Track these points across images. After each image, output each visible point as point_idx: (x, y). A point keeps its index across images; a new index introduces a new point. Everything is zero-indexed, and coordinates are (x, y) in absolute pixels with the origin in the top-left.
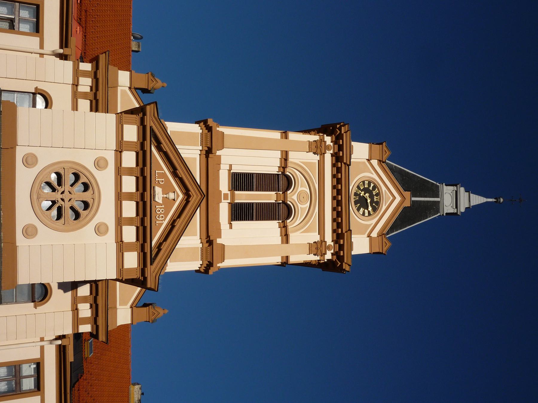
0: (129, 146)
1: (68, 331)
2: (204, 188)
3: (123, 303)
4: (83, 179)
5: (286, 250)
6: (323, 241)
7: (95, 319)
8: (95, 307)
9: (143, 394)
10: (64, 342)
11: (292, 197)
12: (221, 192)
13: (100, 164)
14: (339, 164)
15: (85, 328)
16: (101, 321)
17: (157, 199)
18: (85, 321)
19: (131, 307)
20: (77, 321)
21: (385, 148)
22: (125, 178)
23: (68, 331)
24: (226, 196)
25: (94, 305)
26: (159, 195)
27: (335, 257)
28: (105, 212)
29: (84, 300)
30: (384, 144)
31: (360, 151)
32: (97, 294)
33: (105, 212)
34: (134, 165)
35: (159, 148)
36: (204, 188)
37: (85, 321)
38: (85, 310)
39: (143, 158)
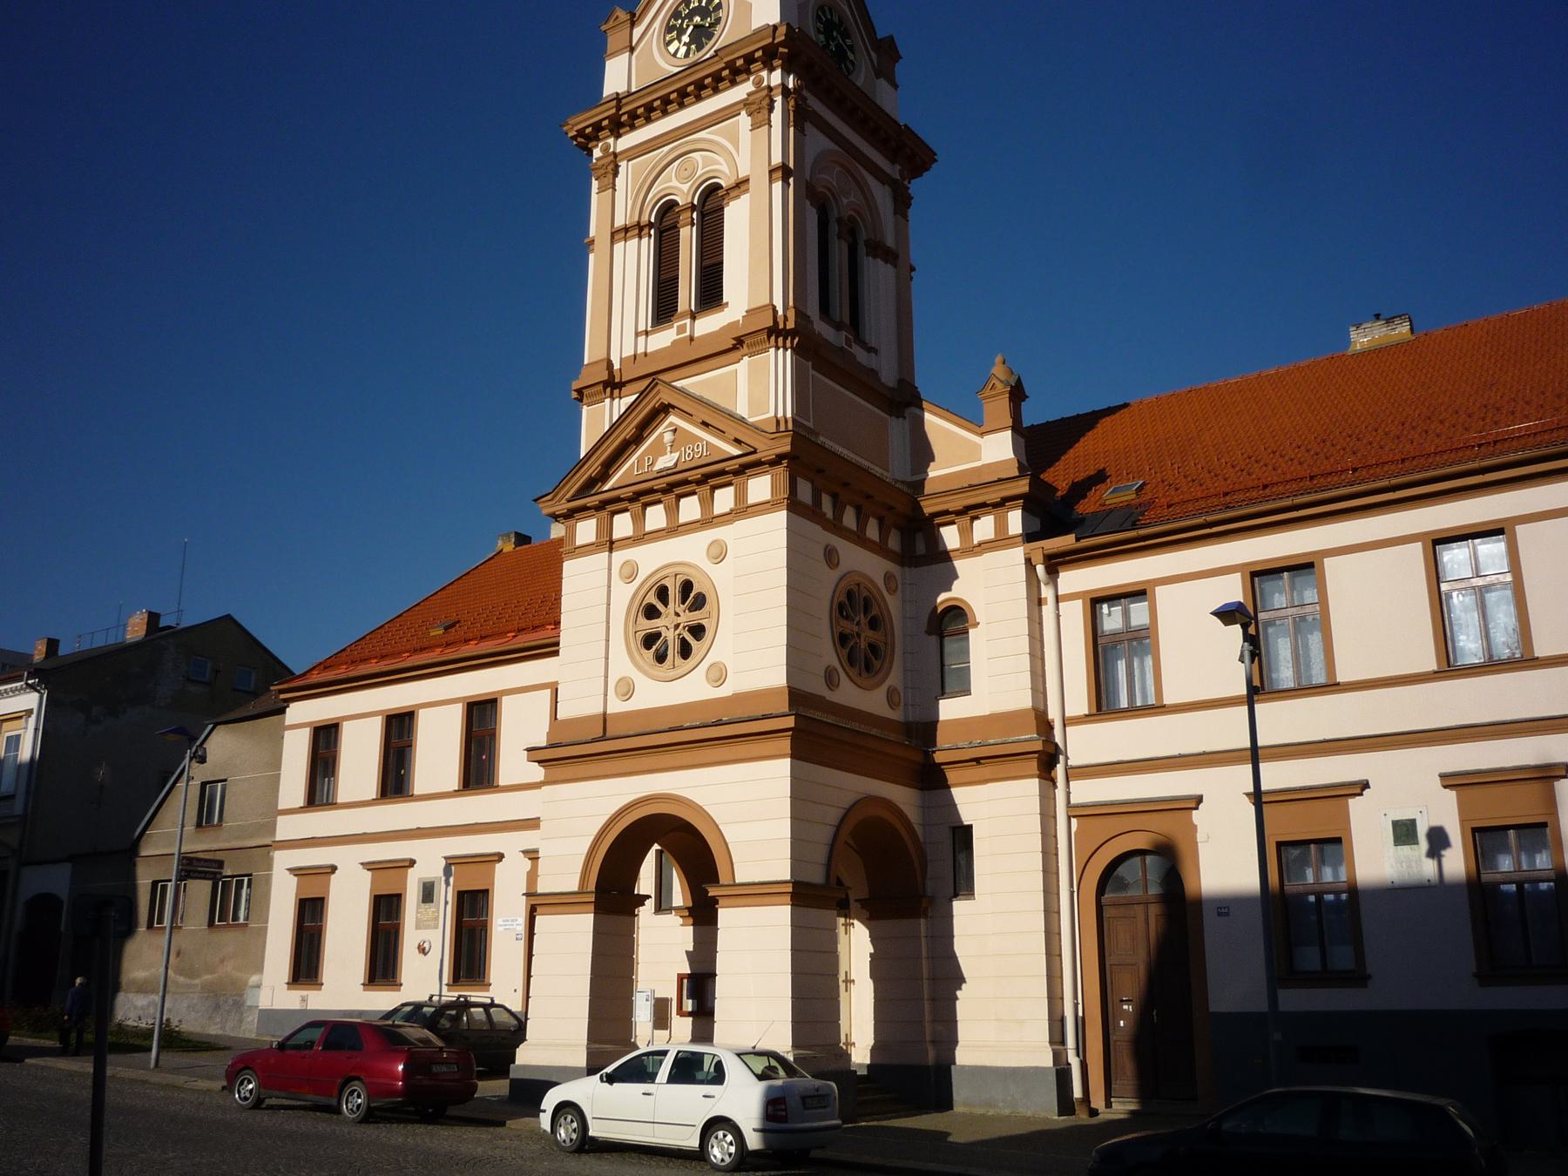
0: (606, 529)
1: (1018, 554)
2: (646, 382)
3: (976, 451)
4: (652, 599)
5: (759, 180)
6: (745, 104)
7: (1002, 504)
8: (971, 512)
9: (1377, 317)
10: (1038, 558)
11: (683, 191)
12: (674, 343)
13: (630, 573)
14: (624, 118)
15: (1015, 520)
16: (993, 495)
17: (671, 464)
18: (1001, 526)
19: (982, 434)
20: (1001, 541)
21: (611, 23)
22: (683, 519)
23: (1018, 554)
24: (681, 330)
25: (972, 513)
26: (666, 461)
27: (777, 62)
28: (688, 552)
29: (966, 533)
30: (603, 28)
31: (617, 76)
32: (946, 513)
33: (688, 552)
34: (627, 515)
35: (604, 476)
36: (646, 382)
37: (1001, 526)
38: (984, 528)
39: (611, 506)
